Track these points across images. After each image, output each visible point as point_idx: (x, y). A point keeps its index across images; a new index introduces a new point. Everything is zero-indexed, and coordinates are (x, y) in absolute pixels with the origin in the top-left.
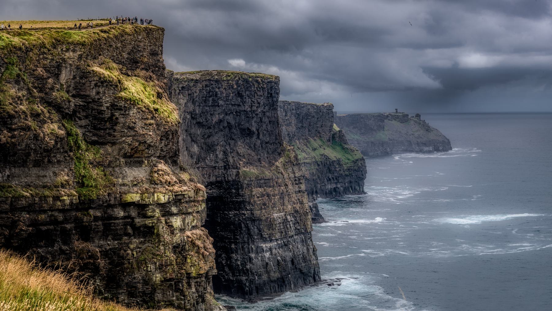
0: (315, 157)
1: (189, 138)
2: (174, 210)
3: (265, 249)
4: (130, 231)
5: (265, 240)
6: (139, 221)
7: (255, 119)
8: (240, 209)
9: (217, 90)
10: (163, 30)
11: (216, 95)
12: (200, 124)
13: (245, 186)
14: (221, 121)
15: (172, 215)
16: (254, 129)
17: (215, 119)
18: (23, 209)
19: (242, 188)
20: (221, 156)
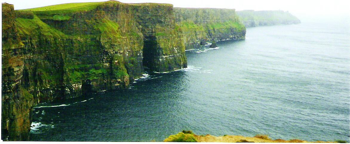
0: (226, 27)
1: (138, 23)
3: (164, 58)
7: (163, 17)
8: (157, 45)
9: (148, 9)
11: (148, 10)
12: (141, 19)
13: (157, 38)
14: (150, 18)
16: (163, 20)
17: (147, 18)
19: (156, 38)
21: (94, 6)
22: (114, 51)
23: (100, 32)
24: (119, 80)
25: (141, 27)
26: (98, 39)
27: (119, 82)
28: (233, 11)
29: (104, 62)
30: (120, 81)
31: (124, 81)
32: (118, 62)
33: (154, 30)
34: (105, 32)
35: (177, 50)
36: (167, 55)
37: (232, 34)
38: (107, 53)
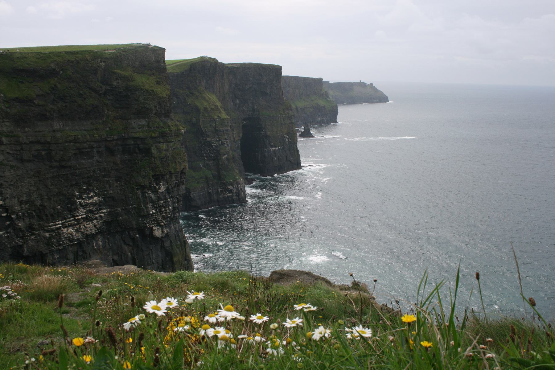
2: (161, 140)
4: (137, 151)
5: (272, 147)
6: (141, 146)
10: (163, 50)
15: (160, 143)
18: (70, 142)
20: (250, 105)
21: (185, 64)
22: (220, 140)
23: (198, 110)
24: (230, 187)
25: (238, 102)
26: (194, 120)
27: (231, 191)
28: (320, 80)
29: (205, 159)
30: (231, 190)
31: (237, 189)
32: (228, 159)
33: (256, 107)
34: (205, 109)
35: (288, 139)
36: (275, 147)
37: (319, 116)
38: (209, 144)
